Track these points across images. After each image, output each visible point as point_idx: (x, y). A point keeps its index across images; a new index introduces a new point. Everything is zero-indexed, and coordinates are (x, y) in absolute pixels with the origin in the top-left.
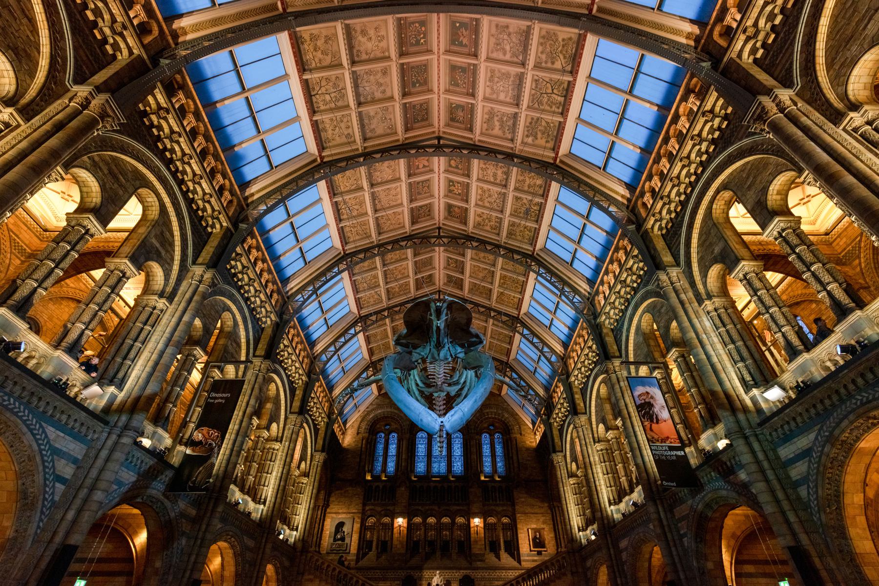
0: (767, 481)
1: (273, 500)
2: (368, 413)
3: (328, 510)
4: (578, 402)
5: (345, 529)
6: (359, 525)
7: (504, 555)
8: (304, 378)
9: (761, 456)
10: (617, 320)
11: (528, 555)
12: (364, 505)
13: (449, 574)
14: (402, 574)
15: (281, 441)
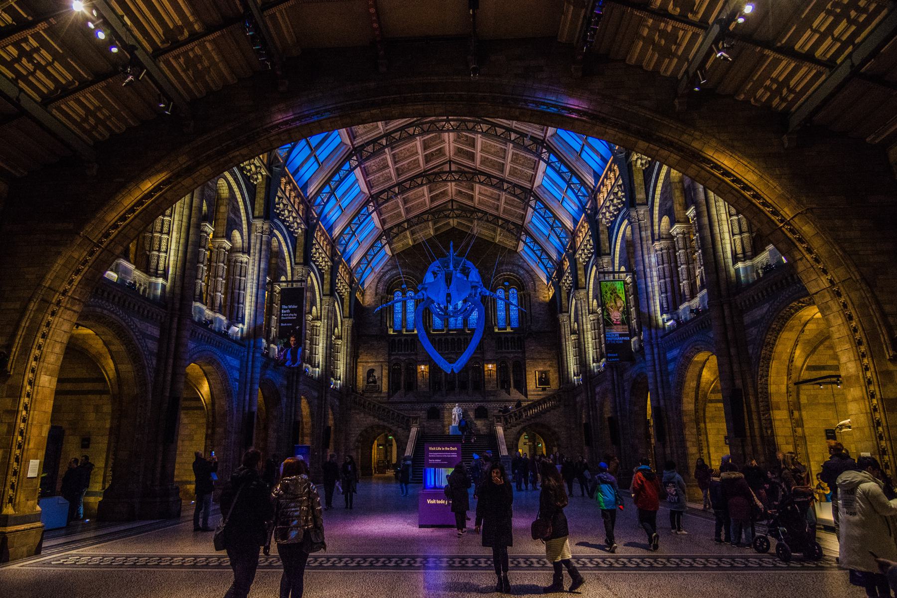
0: (655, 371)
1: (324, 364)
2: (385, 274)
3: (359, 360)
4: (580, 277)
5: (376, 374)
6: (387, 371)
7: (513, 391)
8: (329, 264)
9: (656, 356)
10: (611, 222)
11: (534, 391)
12: (390, 355)
13: (465, 406)
14: (427, 406)
15: (321, 320)
